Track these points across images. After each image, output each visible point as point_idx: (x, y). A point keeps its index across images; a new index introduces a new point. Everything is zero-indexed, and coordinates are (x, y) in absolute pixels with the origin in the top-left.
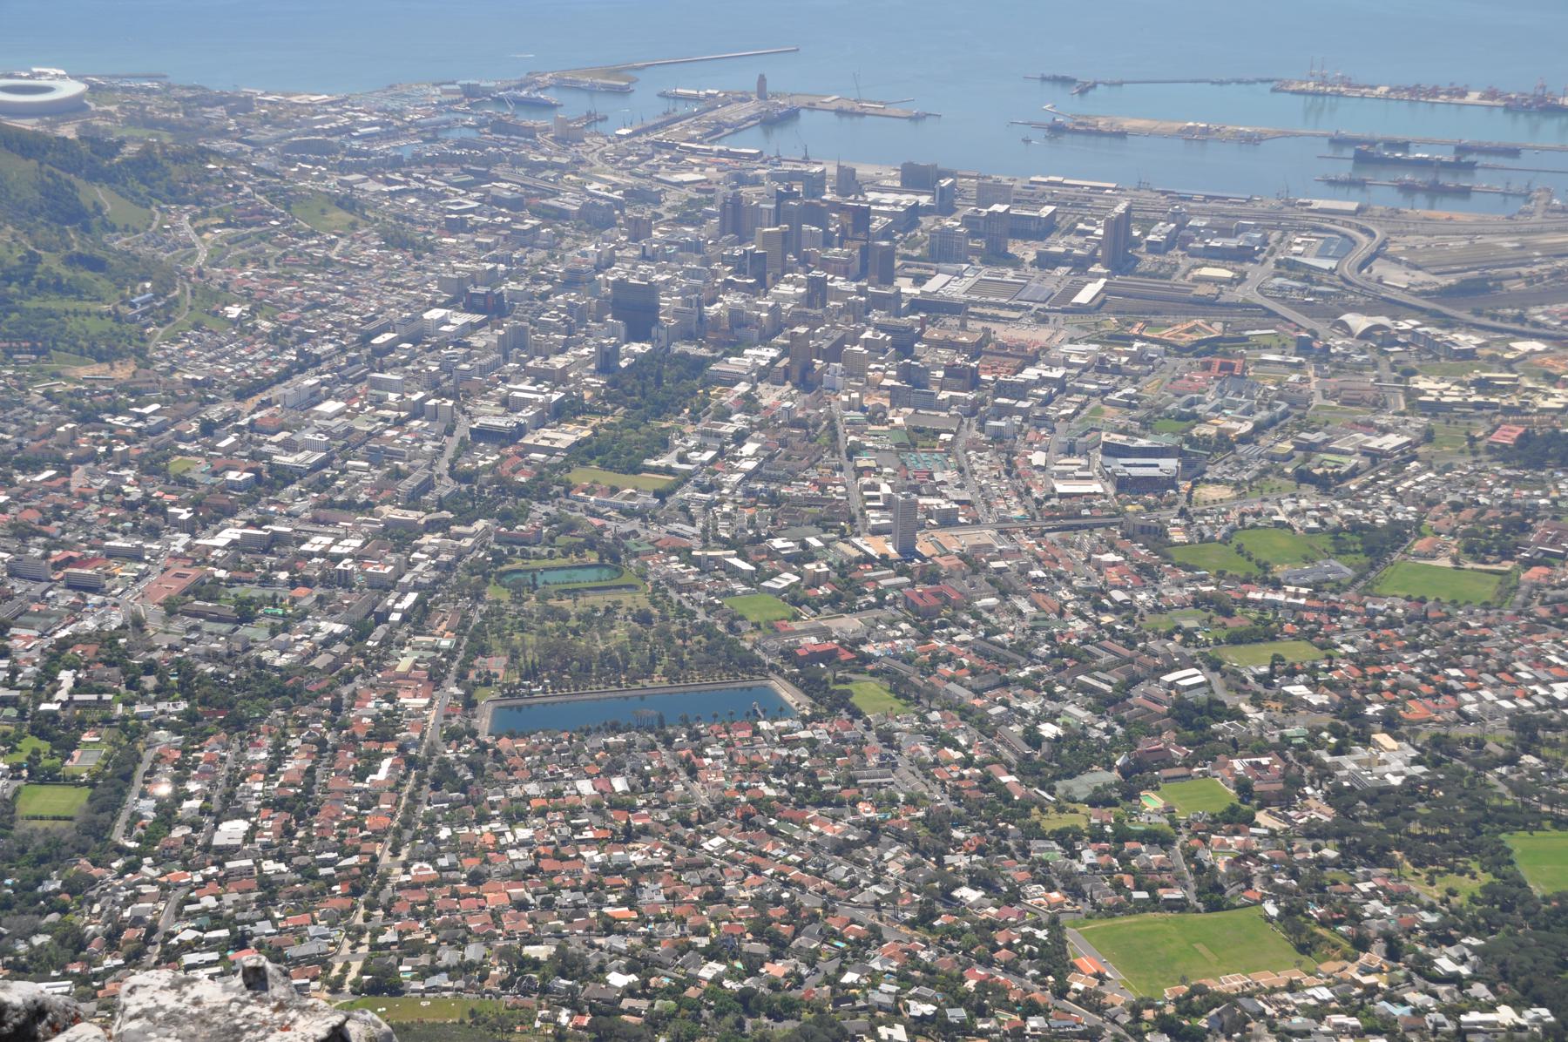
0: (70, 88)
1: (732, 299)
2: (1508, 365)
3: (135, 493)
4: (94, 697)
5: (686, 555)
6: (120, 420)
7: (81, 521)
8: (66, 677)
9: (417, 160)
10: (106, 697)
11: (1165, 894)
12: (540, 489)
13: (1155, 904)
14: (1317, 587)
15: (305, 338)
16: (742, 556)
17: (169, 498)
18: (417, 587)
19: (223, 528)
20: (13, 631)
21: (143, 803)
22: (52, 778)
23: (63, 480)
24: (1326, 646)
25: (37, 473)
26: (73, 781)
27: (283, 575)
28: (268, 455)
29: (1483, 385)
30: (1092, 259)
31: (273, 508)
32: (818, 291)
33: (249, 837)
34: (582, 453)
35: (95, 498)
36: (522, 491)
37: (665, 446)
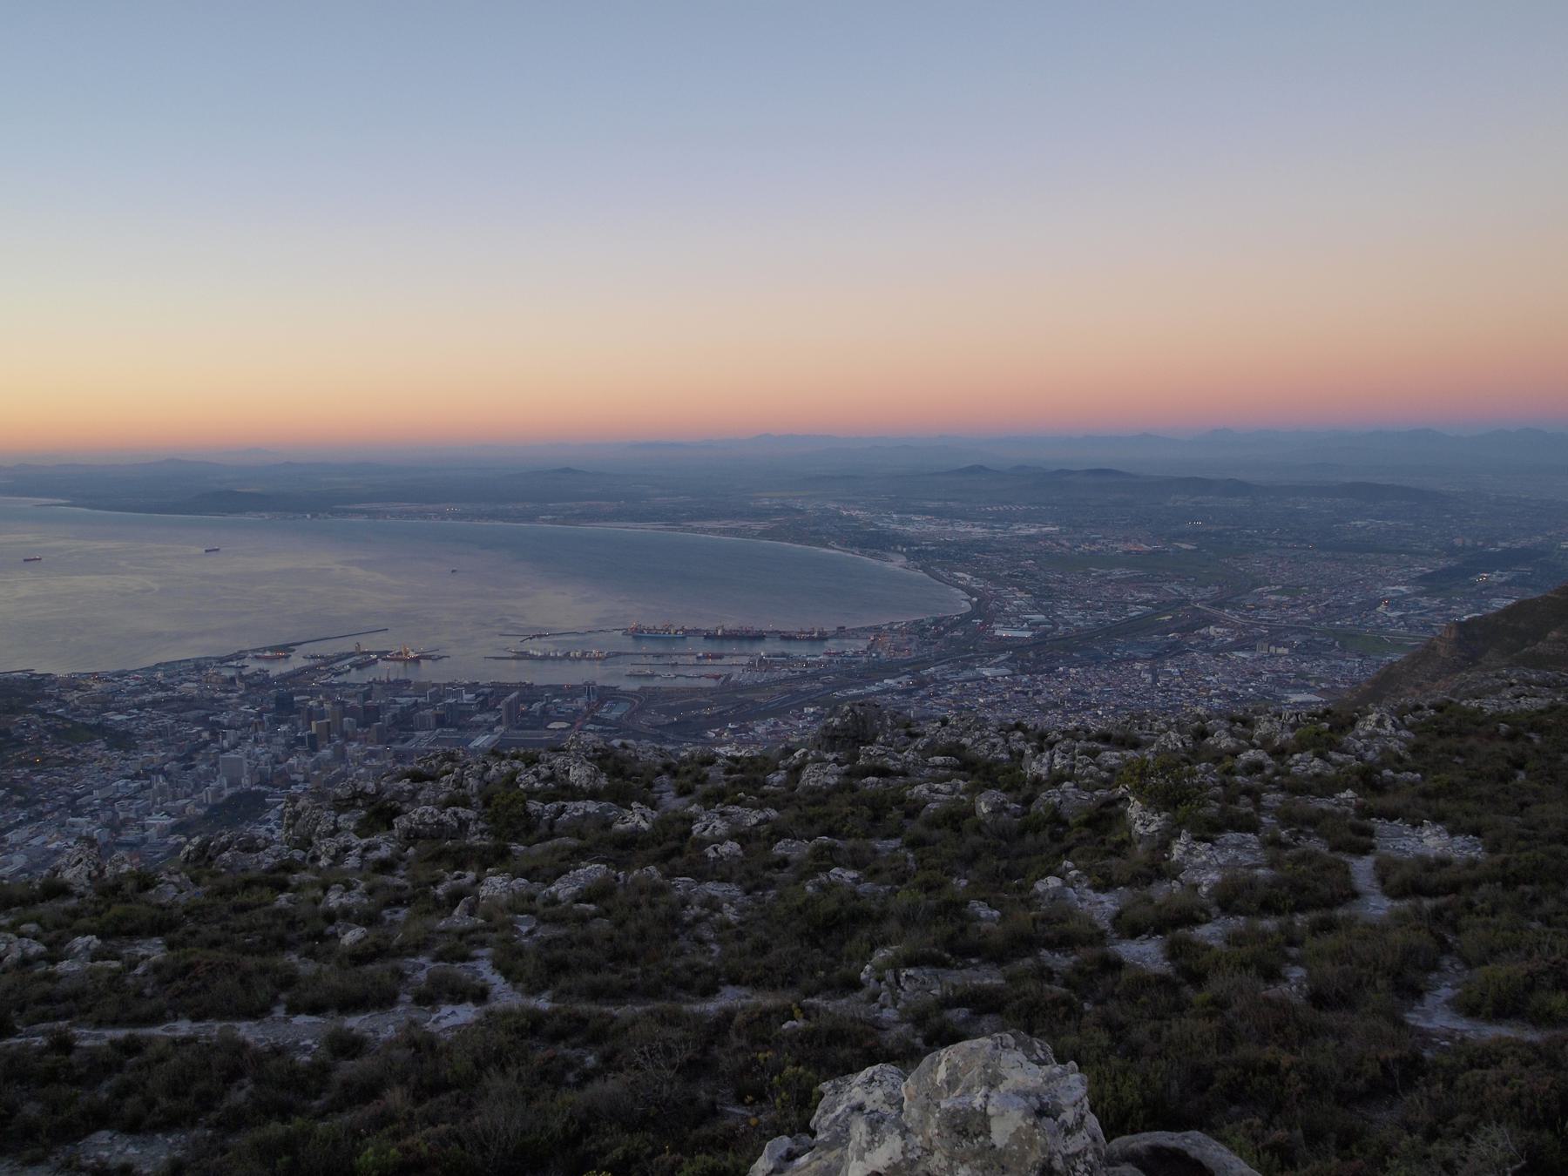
9: (155, 703)
15: (39, 801)
30: (499, 722)
32: (341, 756)
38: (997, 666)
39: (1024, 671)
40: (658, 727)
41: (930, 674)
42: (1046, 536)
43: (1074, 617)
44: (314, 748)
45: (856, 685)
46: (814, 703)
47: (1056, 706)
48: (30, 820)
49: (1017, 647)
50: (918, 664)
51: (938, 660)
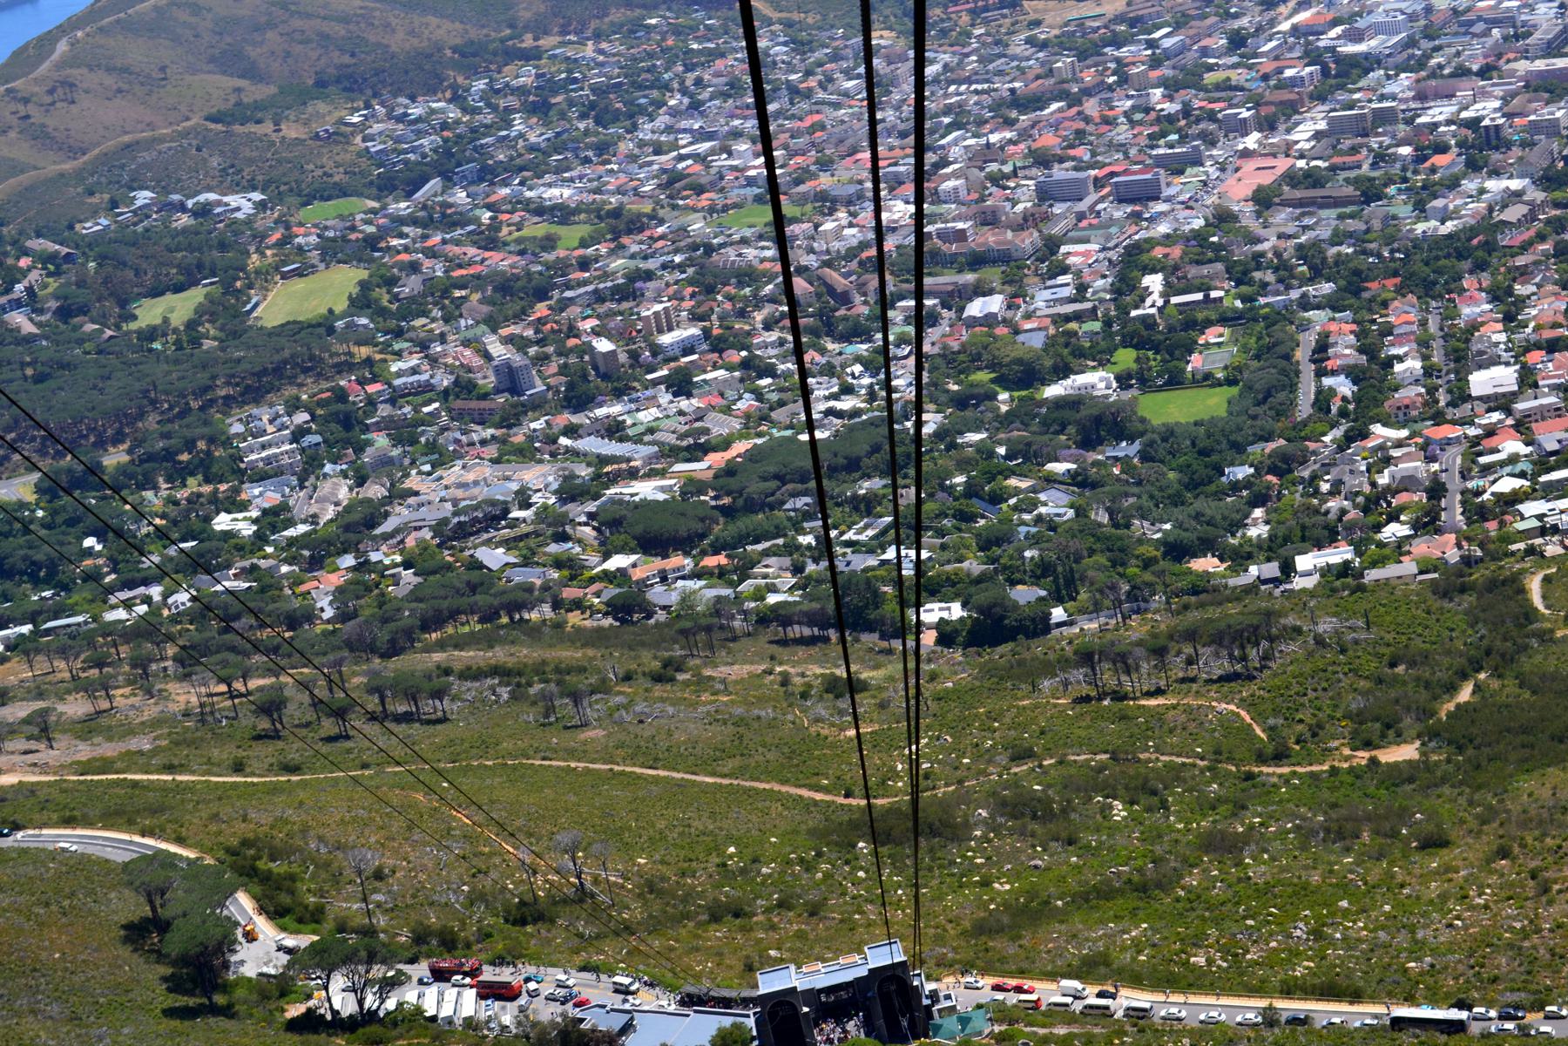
3: (1171, 108)
4: (1199, 296)
6: (1124, 52)
7: (1110, 145)
8: (1154, 282)
10: (1214, 294)
17: (1217, 106)
19: (1297, 124)
20: (1064, 249)
21: (1327, 381)
22: (1175, 381)
23: (1074, 110)
25: (1042, 109)
26: (1206, 380)
27: (1405, 150)
28: (1332, 49)
31: (1357, 96)
35: (1122, 119)
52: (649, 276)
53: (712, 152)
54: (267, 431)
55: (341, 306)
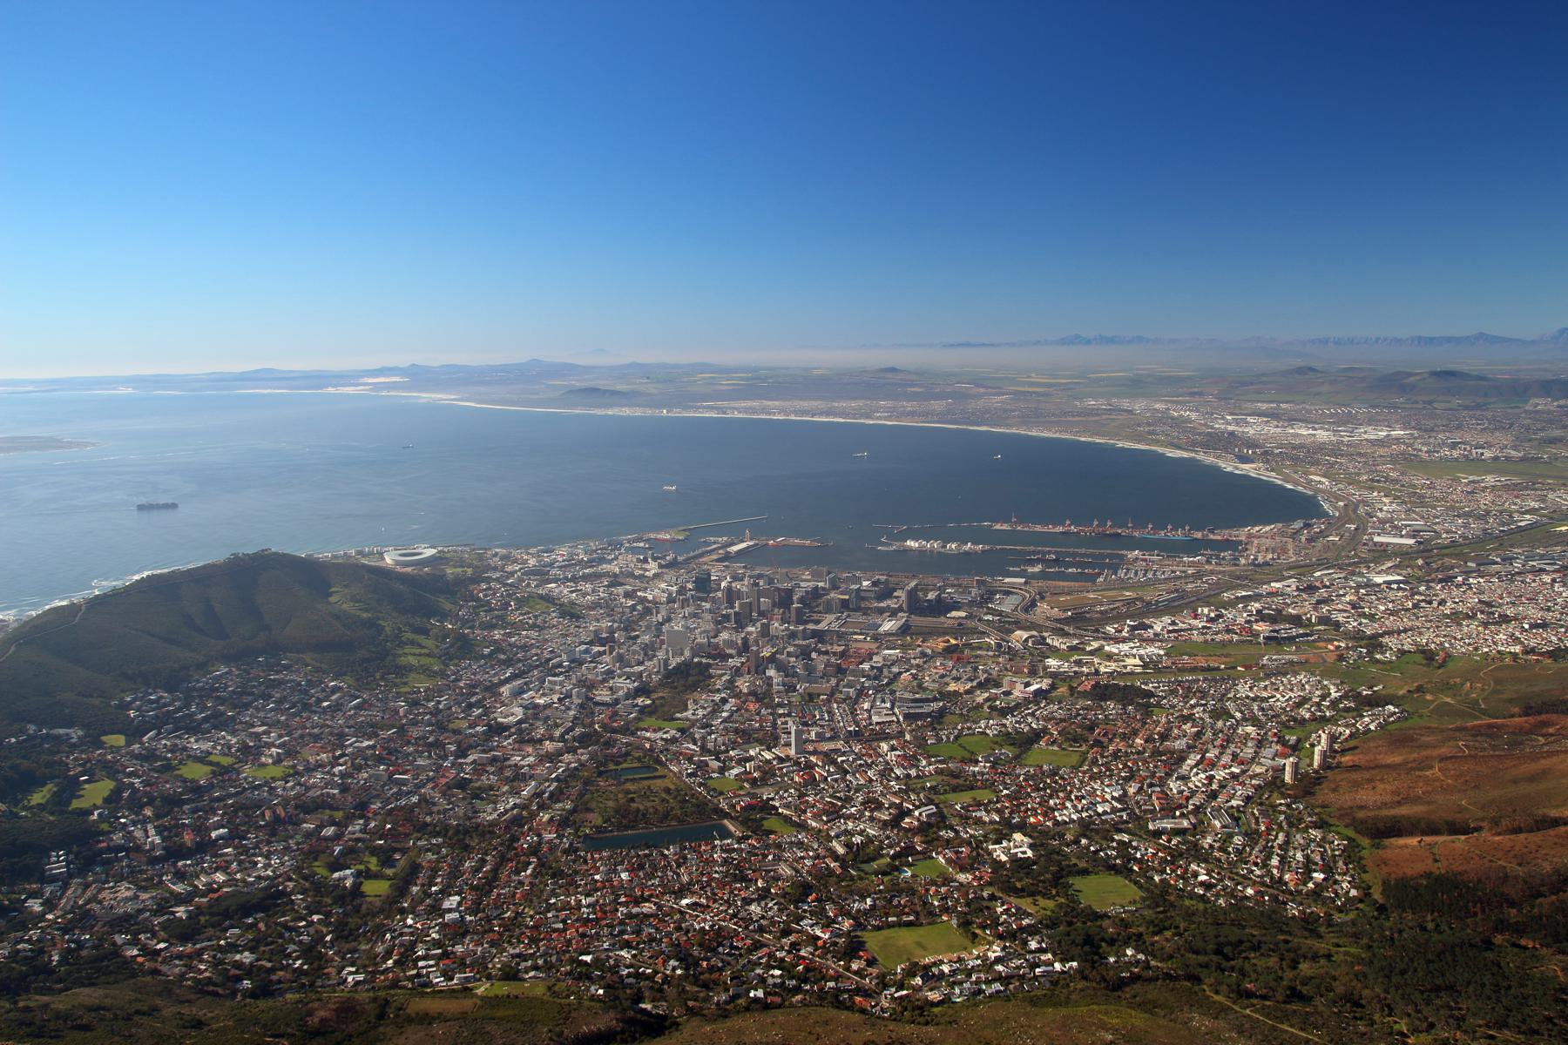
0: (430, 552)
1: (725, 636)
2: (1091, 653)
5: (690, 759)
9: (586, 578)
11: (905, 918)
12: (626, 730)
13: (900, 924)
14: (994, 765)
15: (519, 661)
16: (718, 759)
18: (557, 779)
24: (997, 792)
29: (1079, 663)
30: (900, 609)
32: (765, 632)
33: (460, 904)
34: (643, 711)
36: (614, 731)
37: (686, 709)
38: (1387, 572)
39: (1420, 580)
40: (1058, 621)
41: (1317, 579)
42: (1398, 440)
43: (1452, 529)
44: (740, 626)
45: (1243, 587)
46: (1208, 605)
47: (1468, 617)
48: (514, 677)
49: (1405, 555)
50: (1302, 569)
51: (1322, 564)
52: (219, 799)
53: (264, 733)
54: (58, 863)
55: (99, 802)
